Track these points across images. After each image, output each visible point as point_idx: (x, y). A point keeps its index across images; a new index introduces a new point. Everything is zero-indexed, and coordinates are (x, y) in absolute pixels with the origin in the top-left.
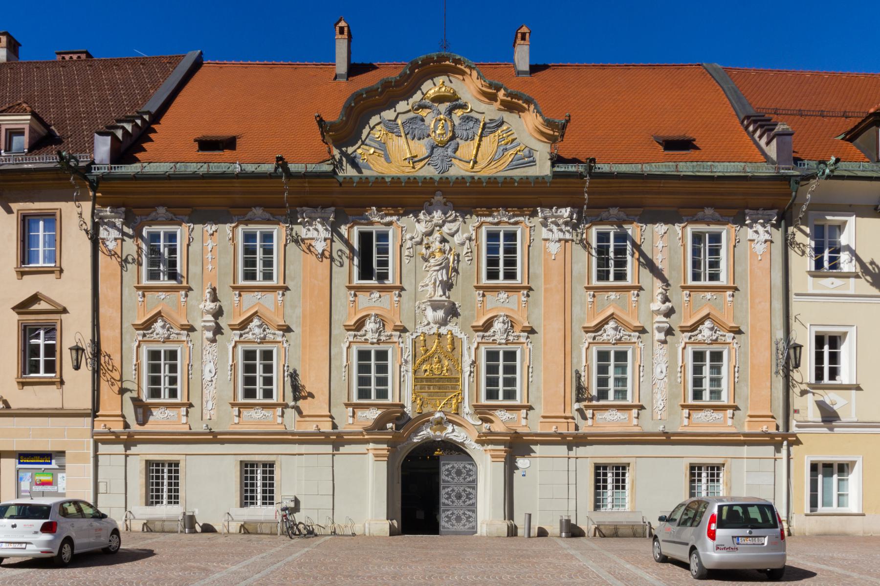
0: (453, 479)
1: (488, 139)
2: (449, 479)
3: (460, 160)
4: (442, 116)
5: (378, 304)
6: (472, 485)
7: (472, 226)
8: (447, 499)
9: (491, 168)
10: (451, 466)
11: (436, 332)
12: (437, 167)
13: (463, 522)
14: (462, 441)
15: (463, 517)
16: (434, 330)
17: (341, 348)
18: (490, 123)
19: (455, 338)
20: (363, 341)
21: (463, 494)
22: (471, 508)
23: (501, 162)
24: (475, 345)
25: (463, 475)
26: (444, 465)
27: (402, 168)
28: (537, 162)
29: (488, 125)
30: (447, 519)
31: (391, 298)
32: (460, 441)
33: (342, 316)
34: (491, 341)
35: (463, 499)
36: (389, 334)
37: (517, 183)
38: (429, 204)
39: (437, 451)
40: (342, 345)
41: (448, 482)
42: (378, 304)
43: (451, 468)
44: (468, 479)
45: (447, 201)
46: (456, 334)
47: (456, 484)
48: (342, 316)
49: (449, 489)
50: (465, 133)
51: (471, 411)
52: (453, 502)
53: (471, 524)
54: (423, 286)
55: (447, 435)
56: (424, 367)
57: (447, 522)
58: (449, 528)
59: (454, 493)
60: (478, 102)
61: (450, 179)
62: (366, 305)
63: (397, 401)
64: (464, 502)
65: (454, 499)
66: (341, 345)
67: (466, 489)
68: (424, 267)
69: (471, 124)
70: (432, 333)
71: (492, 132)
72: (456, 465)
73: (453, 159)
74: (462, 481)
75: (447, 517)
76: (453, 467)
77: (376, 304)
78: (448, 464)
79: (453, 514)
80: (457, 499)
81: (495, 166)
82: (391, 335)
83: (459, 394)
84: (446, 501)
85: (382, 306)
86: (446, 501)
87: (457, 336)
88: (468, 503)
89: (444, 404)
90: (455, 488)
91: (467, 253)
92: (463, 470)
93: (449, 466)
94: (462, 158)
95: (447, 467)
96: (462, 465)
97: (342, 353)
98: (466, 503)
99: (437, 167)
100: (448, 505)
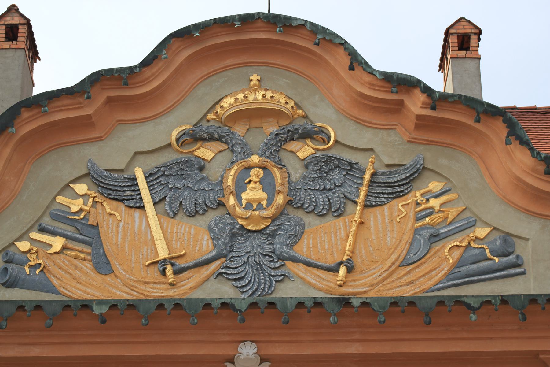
1: (386, 212)
3: (308, 264)
4: (255, 159)
9: (395, 284)
12: (242, 283)
18: (383, 174)
23: (425, 268)
27: (142, 287)
28: (528, 265)
29: (380, 179)
50: (321, 198)
60: (352, 127)
61: (279, 306)
69: (336, 176)
71: (395, 196)
73: (289, 264)
81: (409, 278)
94: (312, 259)
99: (242, 283)
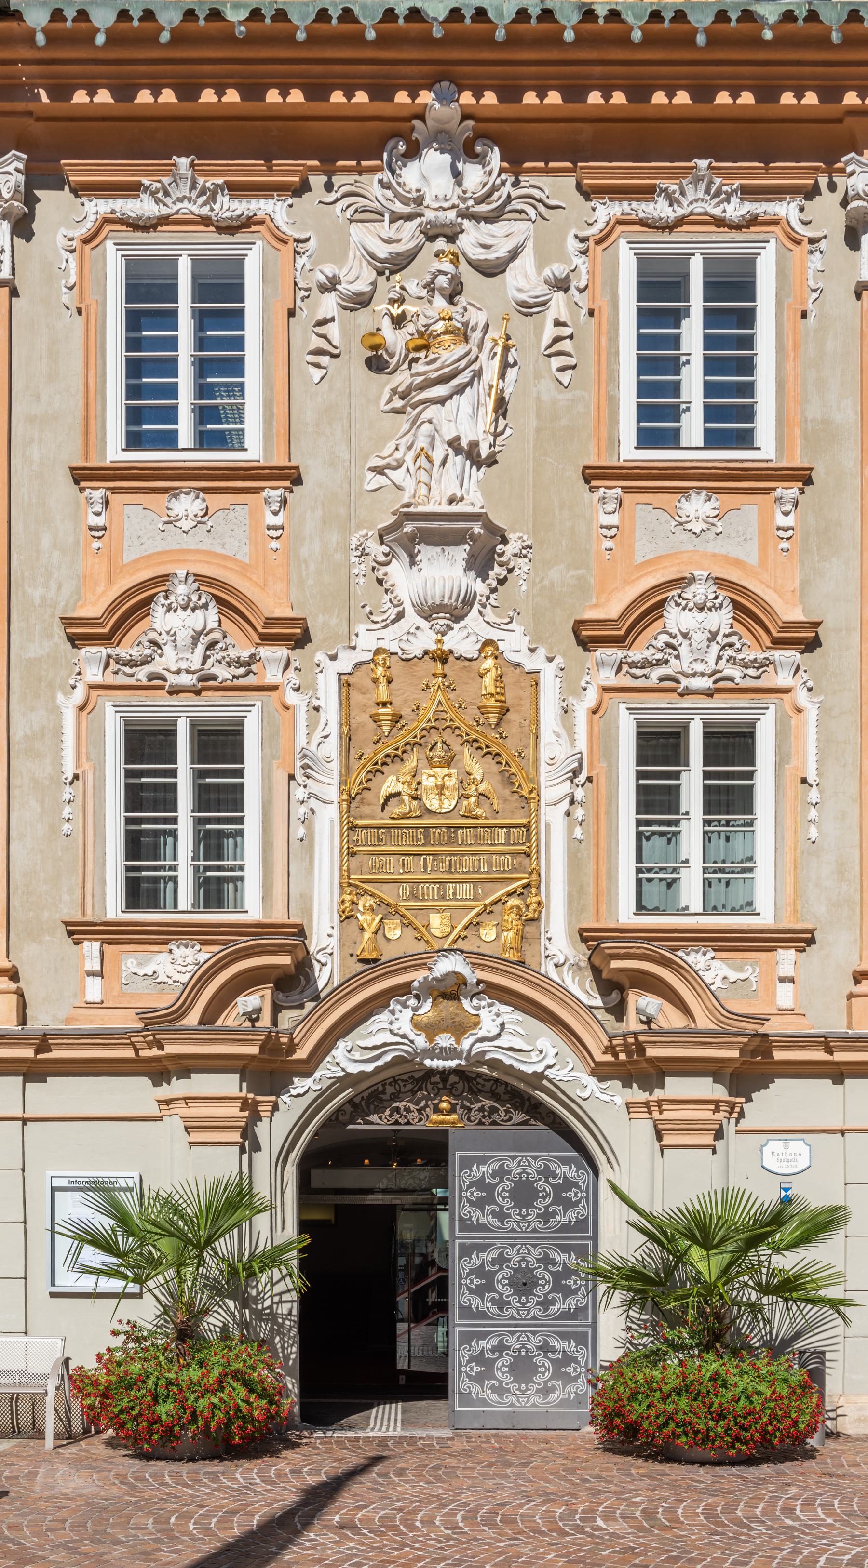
0: (501, 1216)
2: (486, 1218)
5: (198, 541)
6: (576, 1239)
7: (576, 237)
8: (479, 1292)
10: (495, 1167)
11: (433, 647)
13: (539, 1379)
14: (539, 1068)
15: (539, 1360)
16: (426, 640)
17: (57, 712)
19: (509, 671)
20: (144, 681)
21: (540, 1272)
22: (573, 1326)
24: (591, 698)
25: (540, 1204)
26: (466, 1163)
30: (477, 1369)
31: (255, 516)
32: (529, 1069)
33: (59, 588)
34: (653, 681)
35: (540, 1291)
36: (245, 655)
37: (772, 28)
38: (402, 147)
39: (437, 1110)
40: (60, 697)
41: (482, 1227)
42: (198, 541)
43: (494, 1175)
44: (561, 1219)
45: (479, 135)
46: (514, 658)
47: (513, 1238)
48: (59, 588)
49: (488, 1256)
51: (578, 954)
52: (502, 1304)
53: (571, 1388)
54: (379, 471)
55: (480, 1047)
56: (390, 784)
57: (479, 1379)
58: (484, 1402)
59: (507, 1272)
62: (156, 545)
63: (279, 916)
64: (546, 1304)
65: (508, 1291)
66: (54, 698)
67: (552, 1255)
68: (386, 396)
70: (418, 652)
72: (512, 1166)
74: (538, 1224)
75: (479, 1359)
76: (501, 1173)
77: (189, 542)
78: (483, 1161)
79: (500, 1348)
80: (519, 1204)
82: (253, 659)
83: (527, 886)
84: (476, 1302)
85: (219, 550)
86: (476, 1302)
87: (517, 665)
88: (560, 1306)
89: (466, 928)
90: (511, 1253)
91: (557, 340)
92: (540, 1185)
93: (484, 1169)
95: (477, 1171)
96: (537, 1165)
97: (58, 732)
98: (552, 1310)
100: (483, 1315)
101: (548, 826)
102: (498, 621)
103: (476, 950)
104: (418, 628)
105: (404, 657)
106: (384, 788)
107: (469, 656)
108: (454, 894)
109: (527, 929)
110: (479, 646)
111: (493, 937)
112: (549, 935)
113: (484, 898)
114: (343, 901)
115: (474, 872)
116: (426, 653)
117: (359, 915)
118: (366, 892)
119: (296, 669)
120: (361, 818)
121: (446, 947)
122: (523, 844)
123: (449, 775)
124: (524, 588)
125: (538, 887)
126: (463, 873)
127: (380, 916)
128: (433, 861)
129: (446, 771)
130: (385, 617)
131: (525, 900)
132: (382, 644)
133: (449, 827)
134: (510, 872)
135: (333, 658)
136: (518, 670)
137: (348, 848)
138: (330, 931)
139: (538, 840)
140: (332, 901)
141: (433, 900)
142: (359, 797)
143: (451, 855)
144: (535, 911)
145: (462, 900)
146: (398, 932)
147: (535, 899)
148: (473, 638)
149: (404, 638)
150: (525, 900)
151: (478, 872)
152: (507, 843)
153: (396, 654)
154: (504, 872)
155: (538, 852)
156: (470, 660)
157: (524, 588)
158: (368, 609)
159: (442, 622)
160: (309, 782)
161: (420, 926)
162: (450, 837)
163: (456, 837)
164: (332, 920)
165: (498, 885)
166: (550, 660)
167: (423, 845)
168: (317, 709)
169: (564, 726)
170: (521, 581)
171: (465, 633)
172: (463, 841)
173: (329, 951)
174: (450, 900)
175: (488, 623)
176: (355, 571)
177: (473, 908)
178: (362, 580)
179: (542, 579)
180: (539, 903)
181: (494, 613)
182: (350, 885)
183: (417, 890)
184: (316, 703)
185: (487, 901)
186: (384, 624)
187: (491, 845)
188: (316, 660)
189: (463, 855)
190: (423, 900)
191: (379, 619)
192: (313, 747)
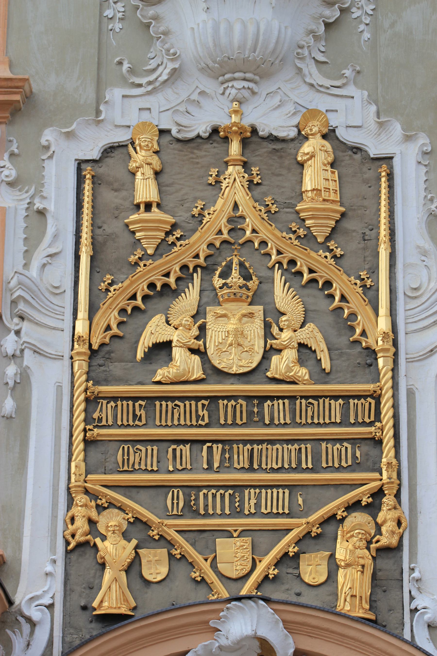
89: (278, 564)
101: (410, 394)
102: (328, 83)
103: (294, 599)
104: (202, 93)
105: (180, 136)
106: (146, 333)
107: (281, 134)
108: (258, 505)
109: (381, 563)
110: (296, 121)
111: (323, 578)
112: (416, 574)
113: (306, 514)
114: (73, 520)
115: (291, 470)
116: (215, 131)
117: (98, 541)
118: (111, 505)
119: (12, 155)
120: (107, 382)
121: (244, 592)
122: (371, 424)
123: (251, 315)
124: (366, 35)
125: (398, 496)
126: (273, 470)
127: (134, 542)
128: (224, 451)
129: (245, 308)
130: (152, 78)
131: (375, 517)
132: (145, 116)
133: (248, 398)
134: (350, 469)
135: (69, 135)
136: (358, 157)
137: (85, 430)
138: (49, 568)
139: (396, 417)
140: (54, 517)
141: (223, 515)
142: (106, 349)
143: (252, 442)
144: (393, 533)
145: (270, 515)
146: (164, 570)
147: (394, 514)
148: (290, 108)
149: (182, 108)
150: (375, 517)
151: (298, 469)
152: (344, 423)
153: (168, 132)
154: (340, 469)
155: (396, 436)
156: (283, 140)
157: (366, 35)
158: (126, 66)
159: (239, 84)
160: (25, 326)
161: (199, 558)
162: (250, 414)
163: (261, 414)
164: (53, 550)
165: (331, 492)
166: (408, 138)
167: (207, 426)
168: (42, 213)
169: (432, 238)
170: (362, 27)
171: (276, 101)
172: (272, 419)
173: (47, 601)
174: (251, 515)
175: (312, 85)
176: (109, 13)
177: (289, 531)
178: (118, 26)
179: (392, 25)
180: (399, 523)
181: (320, 71)
182: (87, 492)
183: (197, 499)
184: (38, 205)
185: (312, 518)
186: (150, 88)
187: (319, 425)
188: (43, 142)
189: (272, 442)
190: (206, 515)
191: (144, 81)
192: (34, 272)
